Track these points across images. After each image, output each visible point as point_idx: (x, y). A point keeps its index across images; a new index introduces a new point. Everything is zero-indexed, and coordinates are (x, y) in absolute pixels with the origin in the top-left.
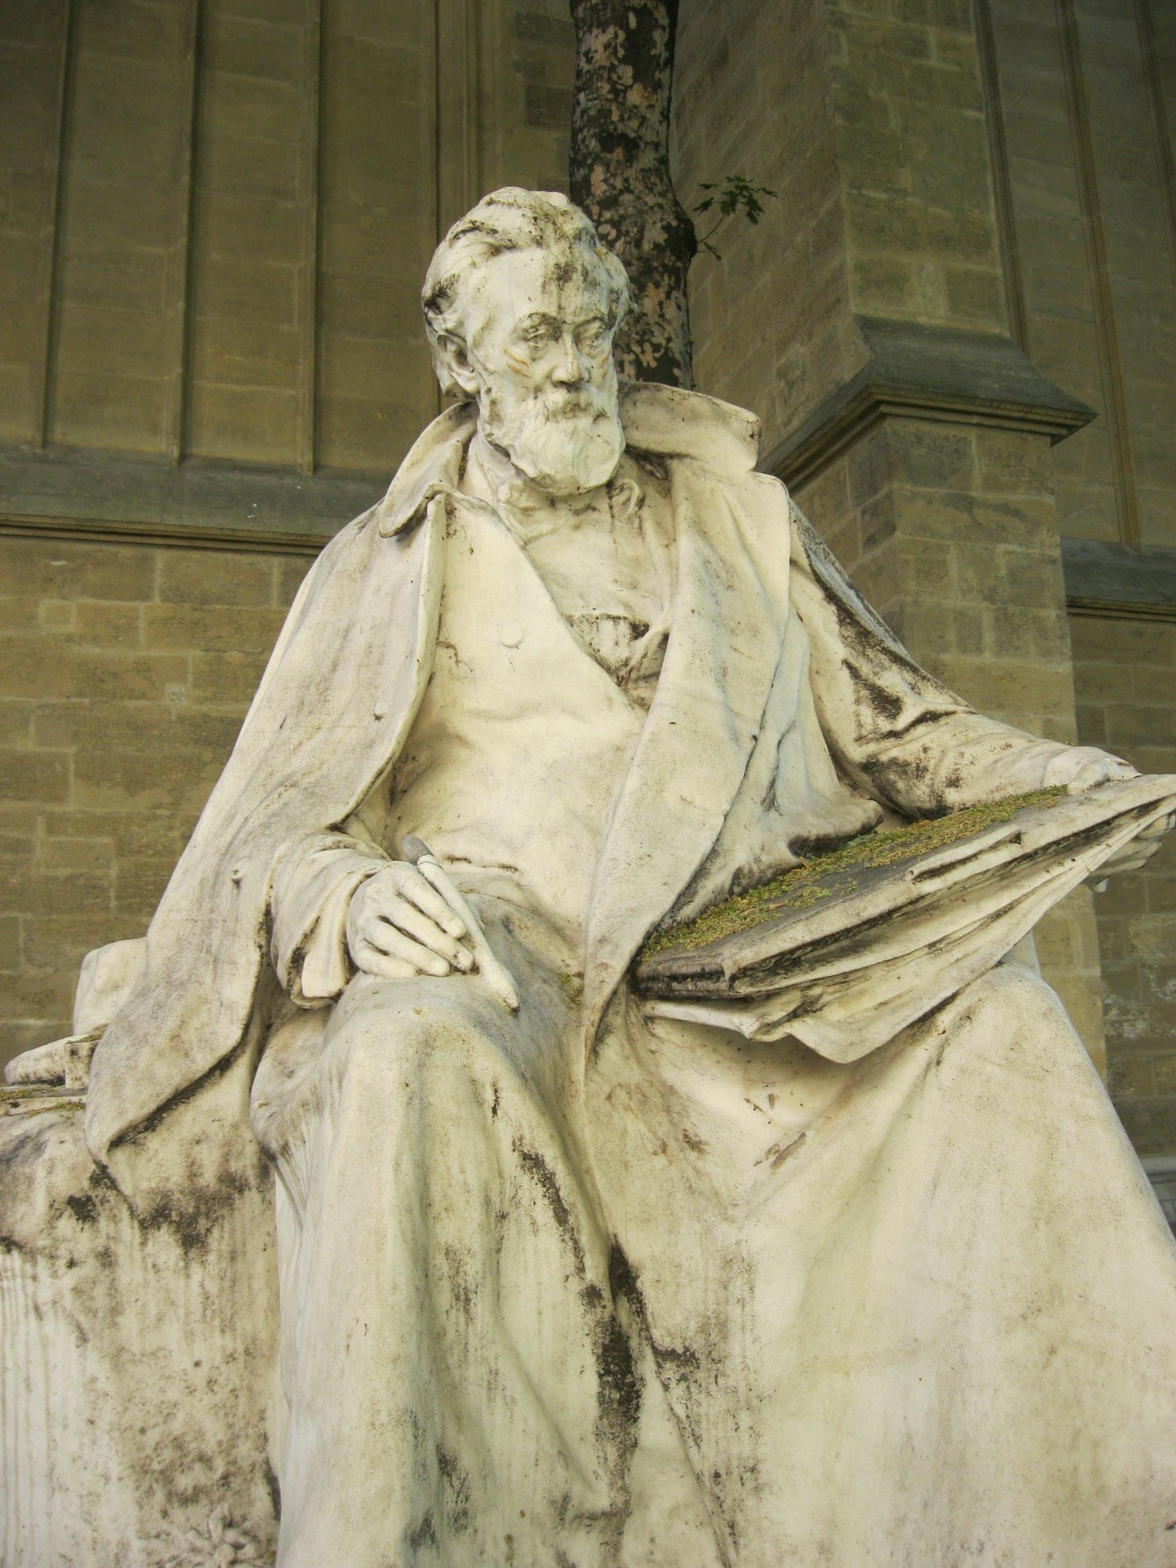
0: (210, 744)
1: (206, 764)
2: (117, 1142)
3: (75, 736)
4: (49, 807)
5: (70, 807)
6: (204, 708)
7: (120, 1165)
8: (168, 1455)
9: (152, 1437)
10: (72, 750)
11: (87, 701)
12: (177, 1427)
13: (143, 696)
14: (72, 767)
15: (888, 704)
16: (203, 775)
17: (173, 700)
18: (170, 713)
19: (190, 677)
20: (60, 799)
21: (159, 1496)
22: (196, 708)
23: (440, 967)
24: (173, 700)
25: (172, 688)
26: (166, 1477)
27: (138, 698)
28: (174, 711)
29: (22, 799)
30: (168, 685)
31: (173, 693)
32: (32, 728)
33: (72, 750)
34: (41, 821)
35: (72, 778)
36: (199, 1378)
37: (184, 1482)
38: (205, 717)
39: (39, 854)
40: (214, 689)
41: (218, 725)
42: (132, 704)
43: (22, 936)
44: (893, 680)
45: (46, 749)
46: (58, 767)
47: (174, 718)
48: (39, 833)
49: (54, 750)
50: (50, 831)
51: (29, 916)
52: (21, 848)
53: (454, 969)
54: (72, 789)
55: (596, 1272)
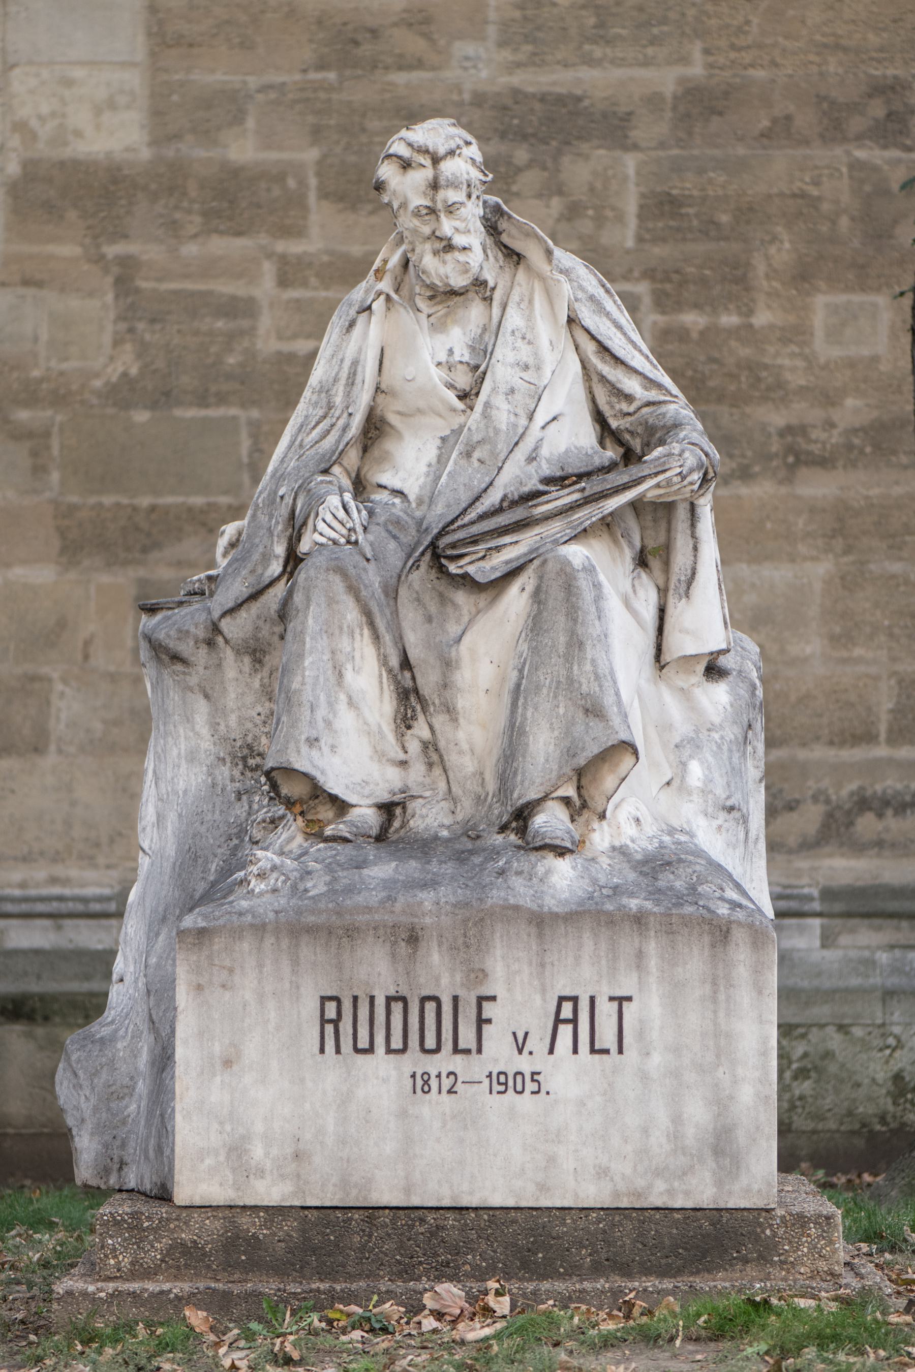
0: (525, 137)
1: (519, 170)
2: (224, 615)
3: (316, 133)
4: (281, 246)
5: (311, 245)
6: (517, 79)
7: (224, 624)
8: (246, 751)
9: (239, 743)
10: (311, 155)
11: (332, 76)
12: (249, 739)
13: (419, 64)
14: (313, 182)
15: (629, 398)
16: (515, 188)
17: (466, 69)
18: (460, 92)
19: (492, 31)
20: (297, 231)
21: (240, 767)
22: (504, 80)
23: (343, 541)
24: (466, 69)
25: (465, 48)
26: (244, 759)
27: (410, 68)
28: (468, 86)
29: (239, 234)
30: (457, 44)
31: (467, 58)
32: (250, 123)
33: (311, 155)
34: (268, 269)
35: (312, 198)
36: (258, 720)
37: (251, 762)
38: (517, 94)
39: (265, 322)
40: (529, 48)
41: (538, 106)
42: (400, 78)
43: (246, 444)
44: (632, 385)
45: (273, 156)
46: (291, 183)
47: (467, 97)
48: (265, 287)
49: (285, 156)
50: (283, 282)
51: (255, 413)
52: (241, 309)
53: (348, 542)
54: (314, 218)
55: (394, 662)
